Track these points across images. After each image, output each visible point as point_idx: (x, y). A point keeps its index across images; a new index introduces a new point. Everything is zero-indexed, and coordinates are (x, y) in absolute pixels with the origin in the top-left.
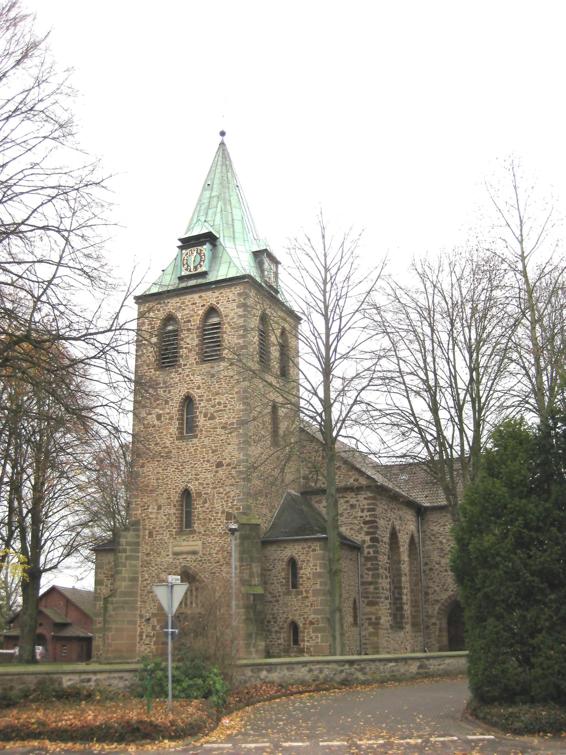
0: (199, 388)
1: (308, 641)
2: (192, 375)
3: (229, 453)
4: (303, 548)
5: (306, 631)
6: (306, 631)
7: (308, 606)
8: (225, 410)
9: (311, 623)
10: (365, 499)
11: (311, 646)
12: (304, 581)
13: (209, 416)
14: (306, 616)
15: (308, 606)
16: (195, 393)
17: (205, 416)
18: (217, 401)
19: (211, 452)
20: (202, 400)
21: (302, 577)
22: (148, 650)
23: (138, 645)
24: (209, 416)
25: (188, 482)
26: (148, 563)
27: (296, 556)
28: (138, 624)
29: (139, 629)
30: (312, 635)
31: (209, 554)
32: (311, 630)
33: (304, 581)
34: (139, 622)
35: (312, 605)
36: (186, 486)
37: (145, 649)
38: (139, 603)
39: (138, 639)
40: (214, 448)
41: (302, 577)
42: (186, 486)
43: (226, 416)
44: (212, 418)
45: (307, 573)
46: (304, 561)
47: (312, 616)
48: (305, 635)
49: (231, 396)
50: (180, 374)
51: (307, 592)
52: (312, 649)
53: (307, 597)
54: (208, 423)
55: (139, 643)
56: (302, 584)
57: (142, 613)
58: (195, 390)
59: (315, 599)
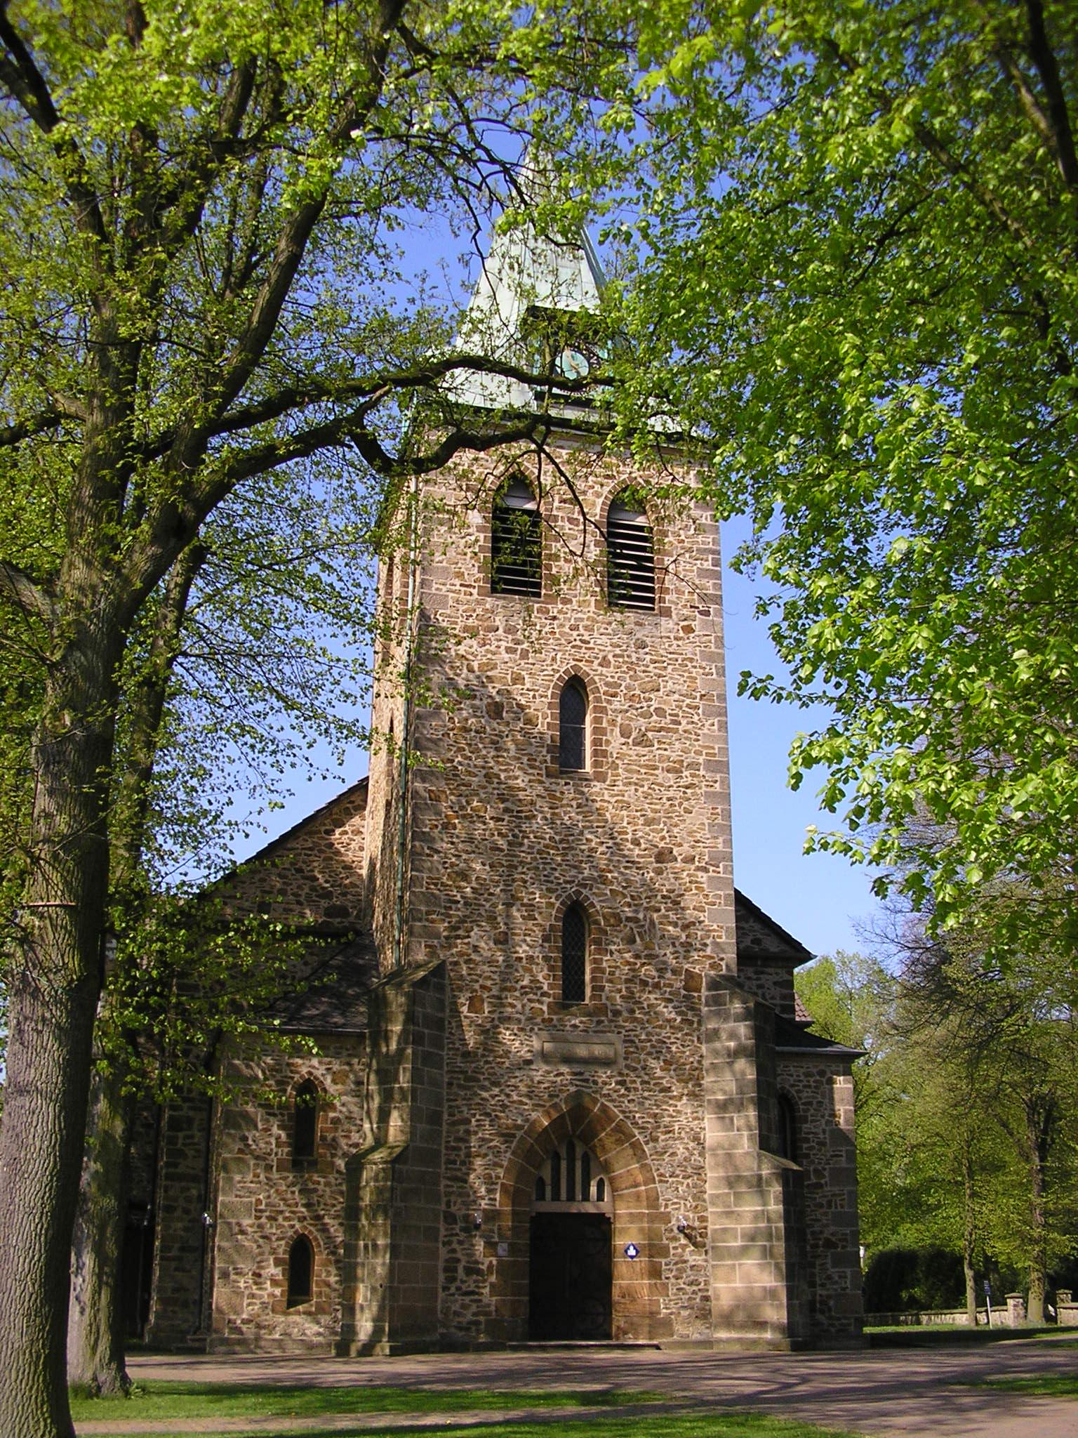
0: (605, 663)
1: (823, 1285)
2: (586, 628)
3: (690, 833)
4: (807, 1075)
5: (818, 1262)
6: (818, 1262)
7: (821, 1206)
8: (676, 731)
9: (829, 1244)
10: (775, 983)
11: (829, 1297)
12: (811, 1148)
13: (634, 735)
14: (817, 1229)
15: (821, 1206)
16: (598, 676)
17: (625, 733)
18: (655, 705)
19: (641, 821)
20: (614, 695)
21: (807, 1140)
22: (474, 1308)
23: (441, 1294)
24: (634, 735)
25: (585, 886)
26: (467, 1079)
27: (793, 1091)
28: (441, 1239)
29: (443, 1252)
30: (831, 1270)
31: (644, 1068)
32: (829, 1260)
33: (811, 1148)
34: (443, 1232)
35: (829, 1203)
36: (578, 893)
37: (464, 1306)
38: (444, 1182)
39: (441, 1277)
40: (651, 815)
41: (807, 1140)
42: (578, 893)
43: (677, 745)
44: (642, 741)
45: (819, 1130)
46: (810, 1103)
47: (832, 1229)
48: (817, 1271)
49: (688, 701)
50: (554, 618)
51: (818, 1173)
52: (832, 1303)
53: (819, 1186)
54: (634, 751)
55: (445, 1289)
56: (807, 1156)
57: (453, 1209)
58: (595, 666)
59: (836, 1189)
